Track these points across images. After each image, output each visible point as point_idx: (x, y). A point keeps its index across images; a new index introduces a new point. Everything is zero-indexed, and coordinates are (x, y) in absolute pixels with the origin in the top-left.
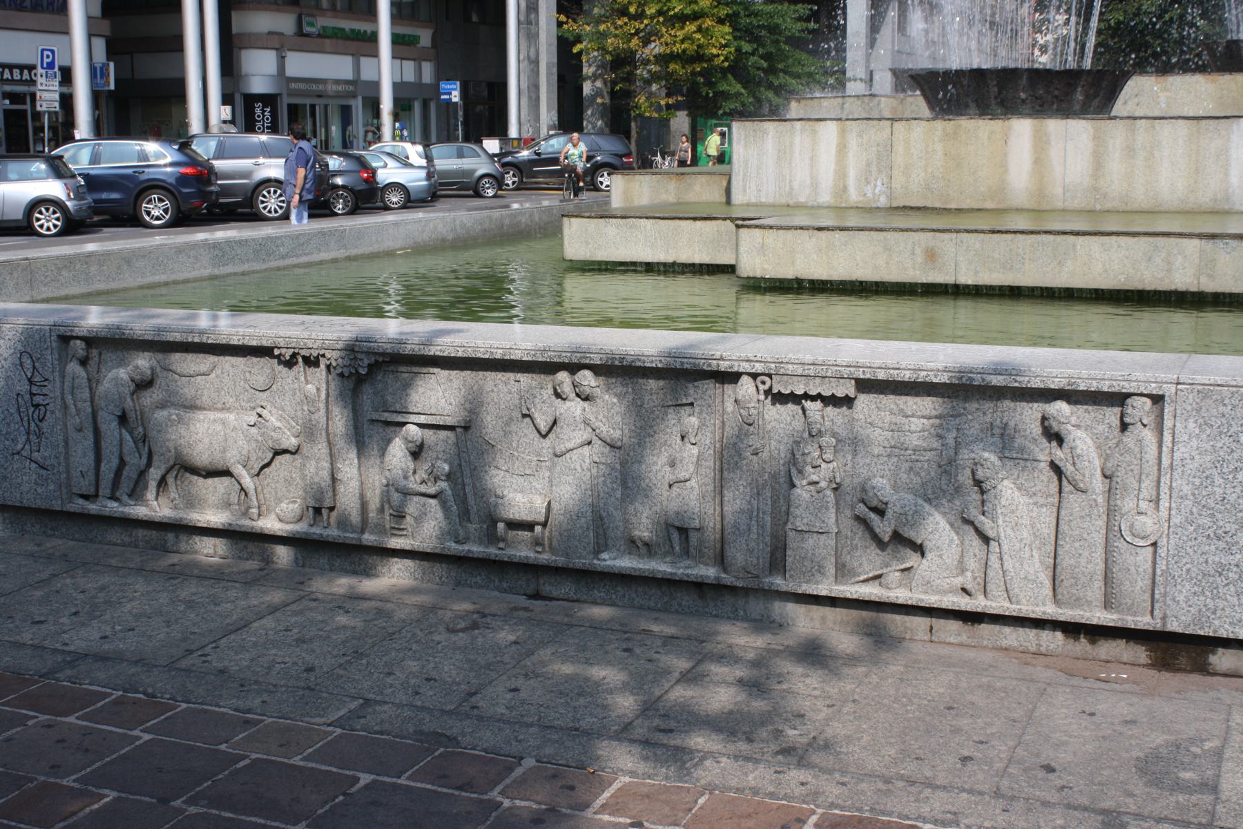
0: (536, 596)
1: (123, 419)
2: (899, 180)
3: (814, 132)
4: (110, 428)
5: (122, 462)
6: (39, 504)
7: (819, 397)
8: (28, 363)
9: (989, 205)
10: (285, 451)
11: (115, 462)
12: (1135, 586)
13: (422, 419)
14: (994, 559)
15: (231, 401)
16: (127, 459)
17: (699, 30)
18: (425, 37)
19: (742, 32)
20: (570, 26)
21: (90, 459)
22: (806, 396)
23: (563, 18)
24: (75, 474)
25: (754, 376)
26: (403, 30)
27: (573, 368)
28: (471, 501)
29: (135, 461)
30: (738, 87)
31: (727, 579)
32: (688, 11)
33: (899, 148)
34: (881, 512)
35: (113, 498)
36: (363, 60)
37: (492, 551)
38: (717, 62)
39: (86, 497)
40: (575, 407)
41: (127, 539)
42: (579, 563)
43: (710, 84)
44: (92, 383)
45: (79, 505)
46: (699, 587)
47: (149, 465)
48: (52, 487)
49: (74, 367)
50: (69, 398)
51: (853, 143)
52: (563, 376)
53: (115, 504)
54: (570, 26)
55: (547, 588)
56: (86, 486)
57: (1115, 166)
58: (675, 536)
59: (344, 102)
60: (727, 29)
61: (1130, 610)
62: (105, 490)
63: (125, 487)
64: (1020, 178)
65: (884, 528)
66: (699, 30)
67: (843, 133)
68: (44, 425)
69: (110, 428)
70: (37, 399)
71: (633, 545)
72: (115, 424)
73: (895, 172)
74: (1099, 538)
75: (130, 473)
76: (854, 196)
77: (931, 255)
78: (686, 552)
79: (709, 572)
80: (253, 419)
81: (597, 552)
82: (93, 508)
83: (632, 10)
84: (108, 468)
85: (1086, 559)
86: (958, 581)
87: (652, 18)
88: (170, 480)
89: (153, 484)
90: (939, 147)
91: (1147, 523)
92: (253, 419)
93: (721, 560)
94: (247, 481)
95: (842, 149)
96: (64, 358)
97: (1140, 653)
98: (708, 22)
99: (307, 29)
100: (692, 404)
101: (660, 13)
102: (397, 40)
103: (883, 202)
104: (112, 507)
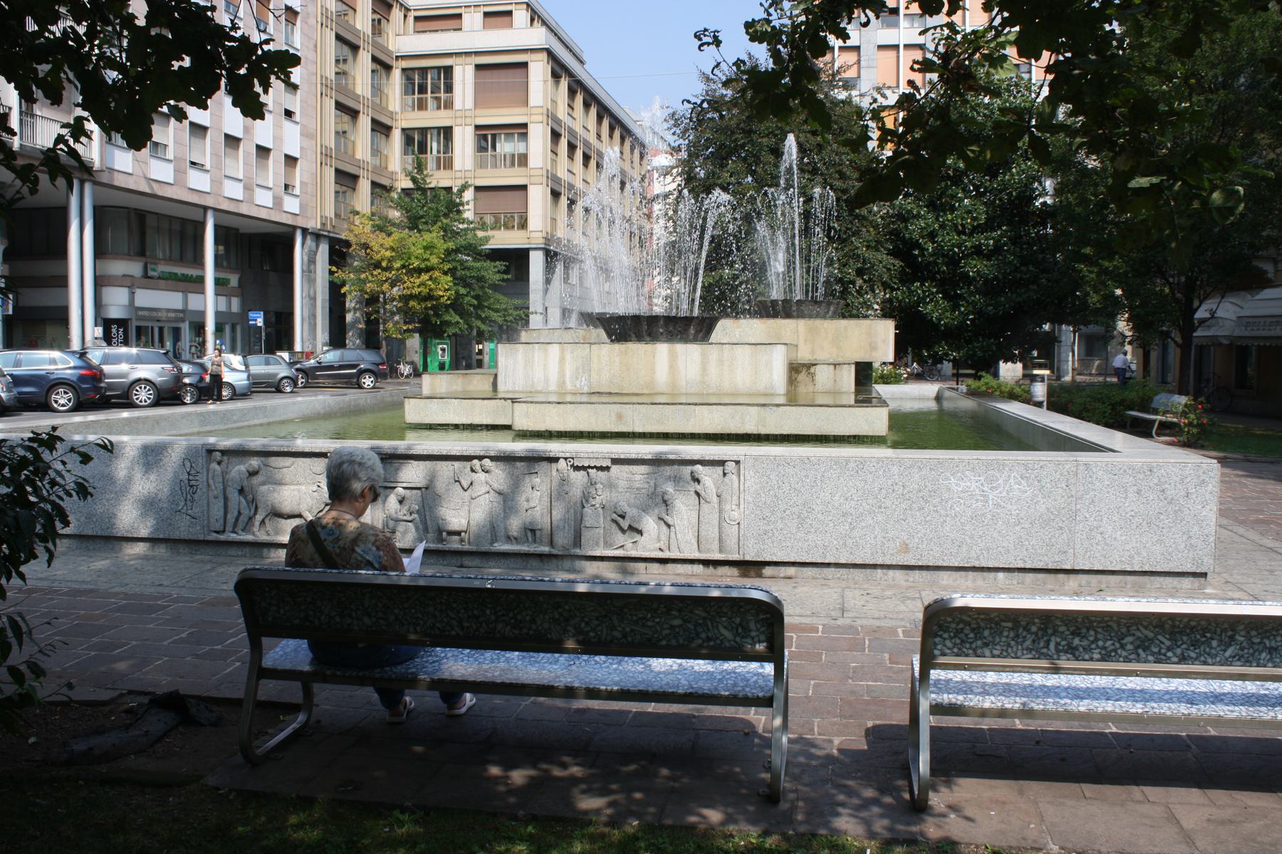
0: (462, 566)
1: (241, 491)
2: (594, 376)
3: (546, 350)
4: (234, 496)
5: (240, 513)
6: (191, 537)
7: (595, 467)
8: (188, 464)
9: (646, 391)
11: (236, 513)
12: (731, 542)
14: (673, 535)
15: (302, 480)
17: (431, 279)
18: (234, 280)
19: (461, 281)
20: (340, 275)
21: (221, 513)
22: (589, 467)
23: (334, 269)
24: (212, 520)
26: (222, 275)
27: (480, 458)
28: (429, 522)
29: (246, 512)
30: (457, 318)
31: (555, 552)
32: (423, 266)
33: (595, 360)
34: (623, 517)
36: (191, 296)
37: (440, 546)
38: (442, 300)
42: (483, 549)
43: (437, 315)
44: (224, 473)
45: (214, 537)
46: (540, 556)
47: (255, 513)
49: (214, 466)
50: (211, 482)
51: (568, 356)
52: (476, 462)
53: (234, 535)
54: (340, 275)
56: (219, 526)
57: (713, 370)
58: (529, 534)
59: (175, 325)
60: (449, 278)
61: (730, 552)
62: (229, 528)
63: (240, 525)
64: (662, 376)
65: (625, 524)
66: (431, 279)
67: (562, 351)
68: (196, 496)
69: (234, 496)
71: (509, 539)
72: (236, 494)
73: (593, 373)
74: (716, 522)
75: (243, 519)
76: (569, 387)
77: (620, 417)
78: (535, 541)
79: (546, 549)
80: (315, 488)
81: (492, 544)
82: (222, 537)
83: (384, 264)
84: (231, 517)
85: (711, 532)
86: (658, 545)
87: (398, 270)
88: (267, 521)
89: (257, 524)
90: (617, 359)
91: (735, 515)
92: (315, 488)
93: (552, 544)
95: (562, 360)
96: (209, 461)
97: (734, 571)
98: (437, 274)
99: (151, 273)
101: (403, 266)
102: (219, 282)
103: (586, 390)
104: (233, 537)
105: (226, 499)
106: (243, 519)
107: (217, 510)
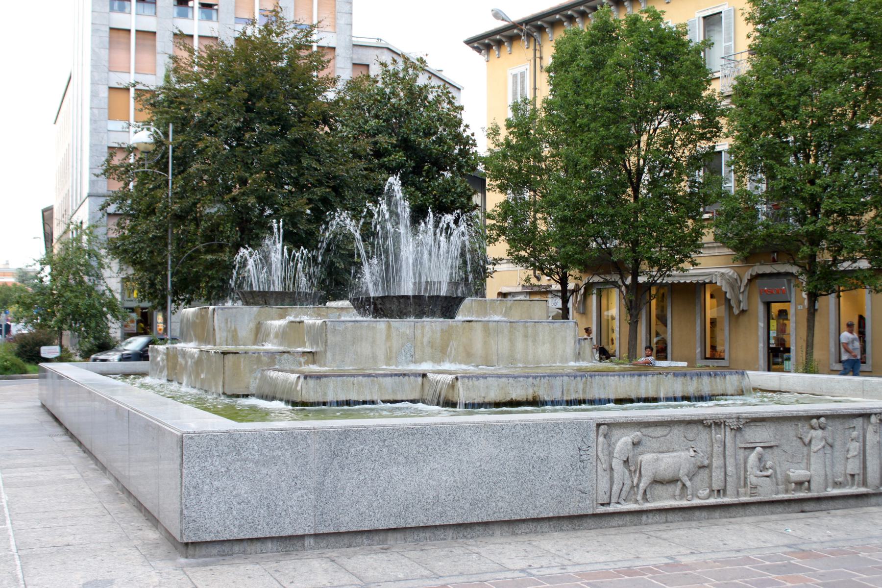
1: (626, 462)
10: (704, 467)
13: (762, 445)
15: (677, 447)
16: (625, 482)
21: (608, 486)
24: (601, 493)
25: (876, 414)
27: (818, 417)
35: (618, 503)
39: (602, 505)
40: (819, 433)
41: (621, 523)
44: (610, 446)
45: (601, 510)
48: (588, 502)
52: (815, 421)
53: (619, 506)
55: (806, 508)
58: (849, 478)
62: (614, 500)
70: (584, 457)
71: (837, 484)
82: (611, 509)
84: (616, 488)
89: (641, 491)
94: (688, 484)
100: (854, 427)
105: (612, 469)
106: (626, 488)
107: (604, 484)
